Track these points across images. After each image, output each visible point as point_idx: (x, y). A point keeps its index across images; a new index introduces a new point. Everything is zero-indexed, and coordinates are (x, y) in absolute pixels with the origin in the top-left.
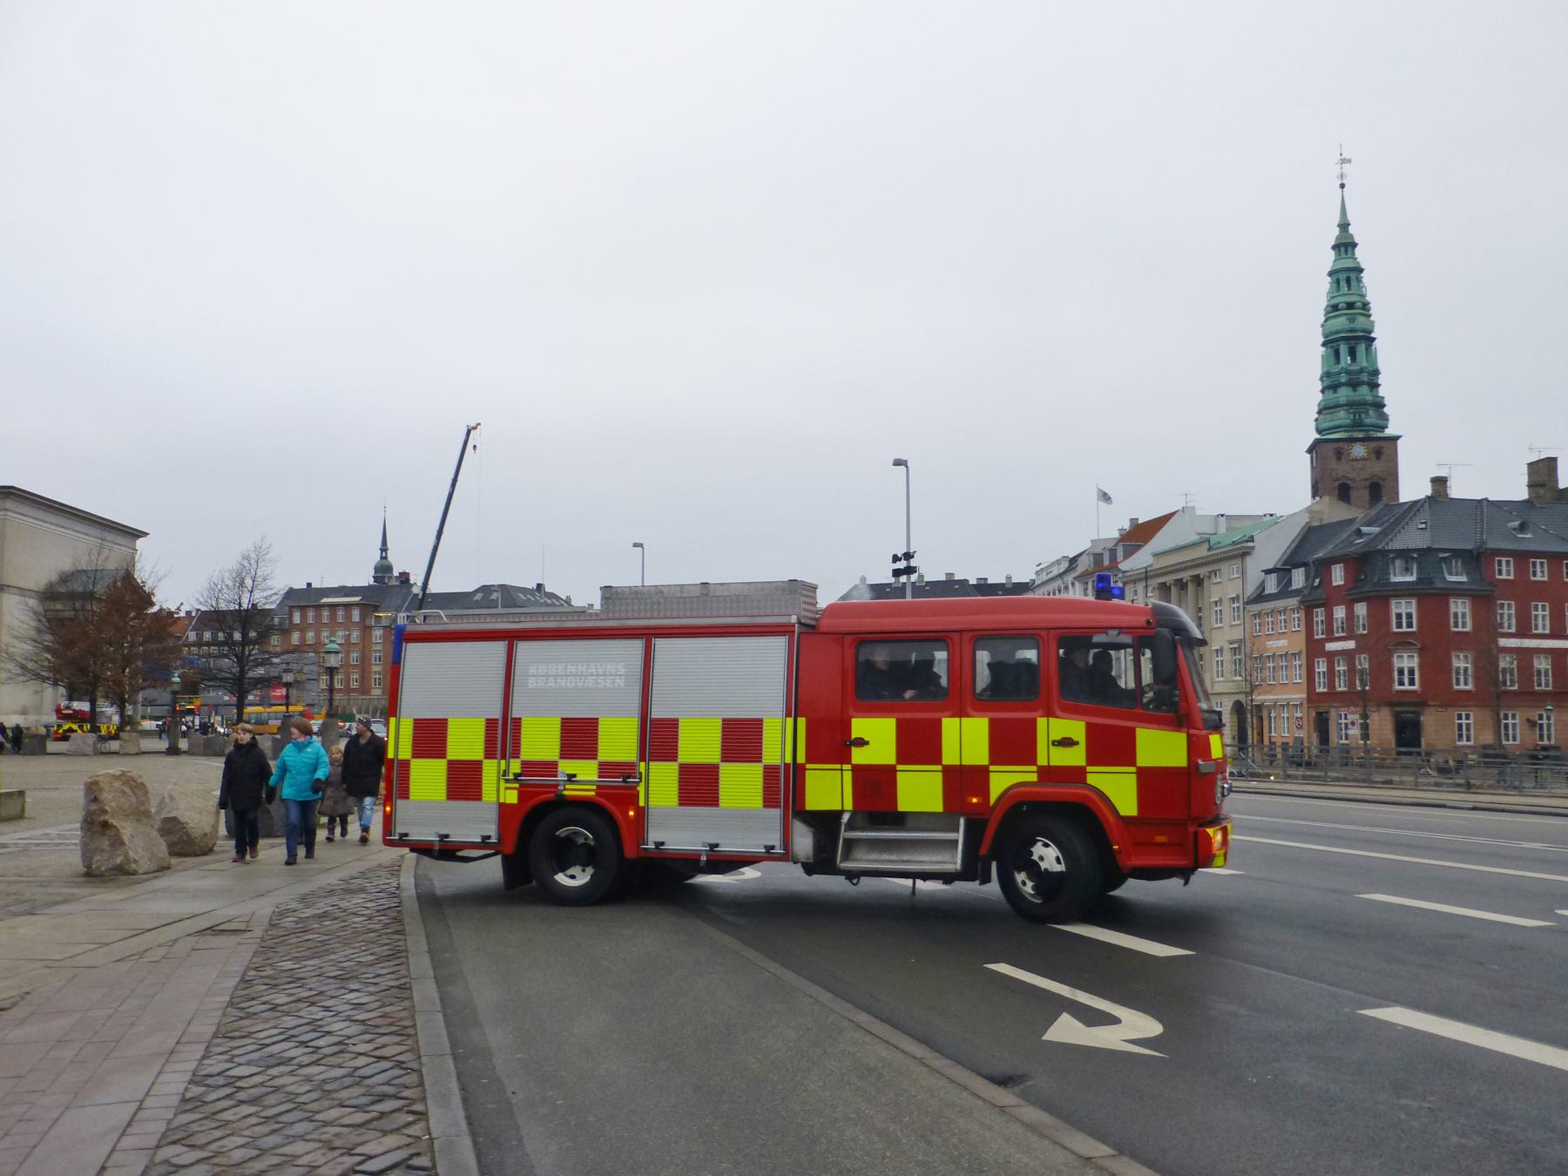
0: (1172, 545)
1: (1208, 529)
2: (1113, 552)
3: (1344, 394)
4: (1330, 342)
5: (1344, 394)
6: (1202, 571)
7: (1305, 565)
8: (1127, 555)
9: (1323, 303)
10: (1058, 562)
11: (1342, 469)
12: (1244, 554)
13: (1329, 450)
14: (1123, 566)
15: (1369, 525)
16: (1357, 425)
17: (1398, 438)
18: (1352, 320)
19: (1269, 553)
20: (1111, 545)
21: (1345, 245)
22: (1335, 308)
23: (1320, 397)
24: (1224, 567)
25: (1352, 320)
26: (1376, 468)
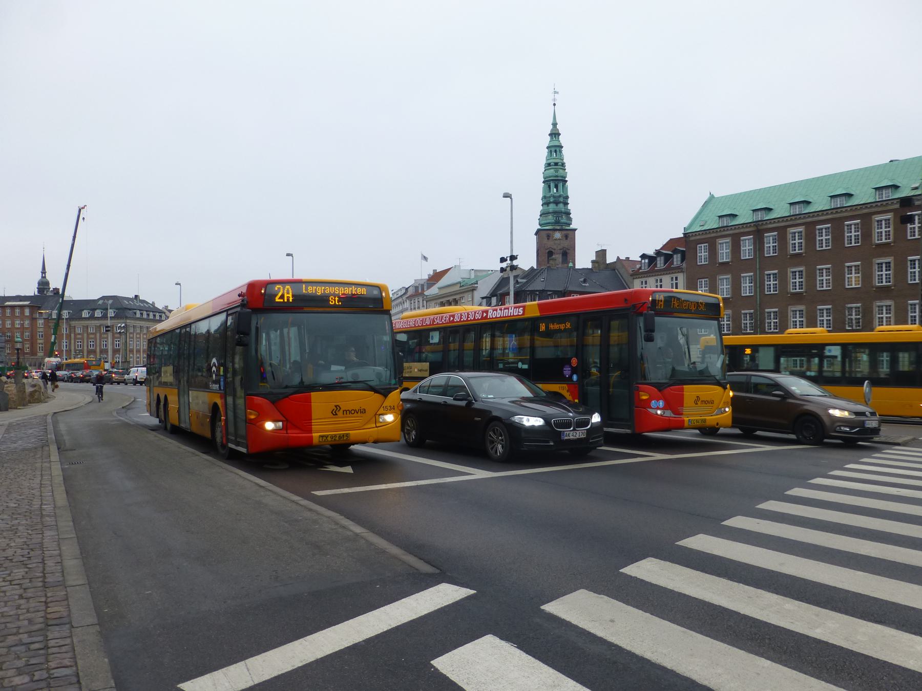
0: (449, 283)
1: (466, 276)
2: (423, 286)
3: (552, 207)
4: (546, 182)
5: (552, 207)
6: (457, 297)
7: (496, 295)
8: (429, 288)
9: (544, 162)
10: (401, 290)
11: (550, 244)
12: (473, 290)
13: (544, 234)
14: (426, 293)
15: (523, 278)
16: (557, 222)
17: (575, 230)
18: (557, 172)
19: (485, 288)
20: (422, 282)
21: (555, 134)
22: (549, 165)
23: (541, 208)
24: (465, 295)
25: (557, 172)
26: (565, 244)
